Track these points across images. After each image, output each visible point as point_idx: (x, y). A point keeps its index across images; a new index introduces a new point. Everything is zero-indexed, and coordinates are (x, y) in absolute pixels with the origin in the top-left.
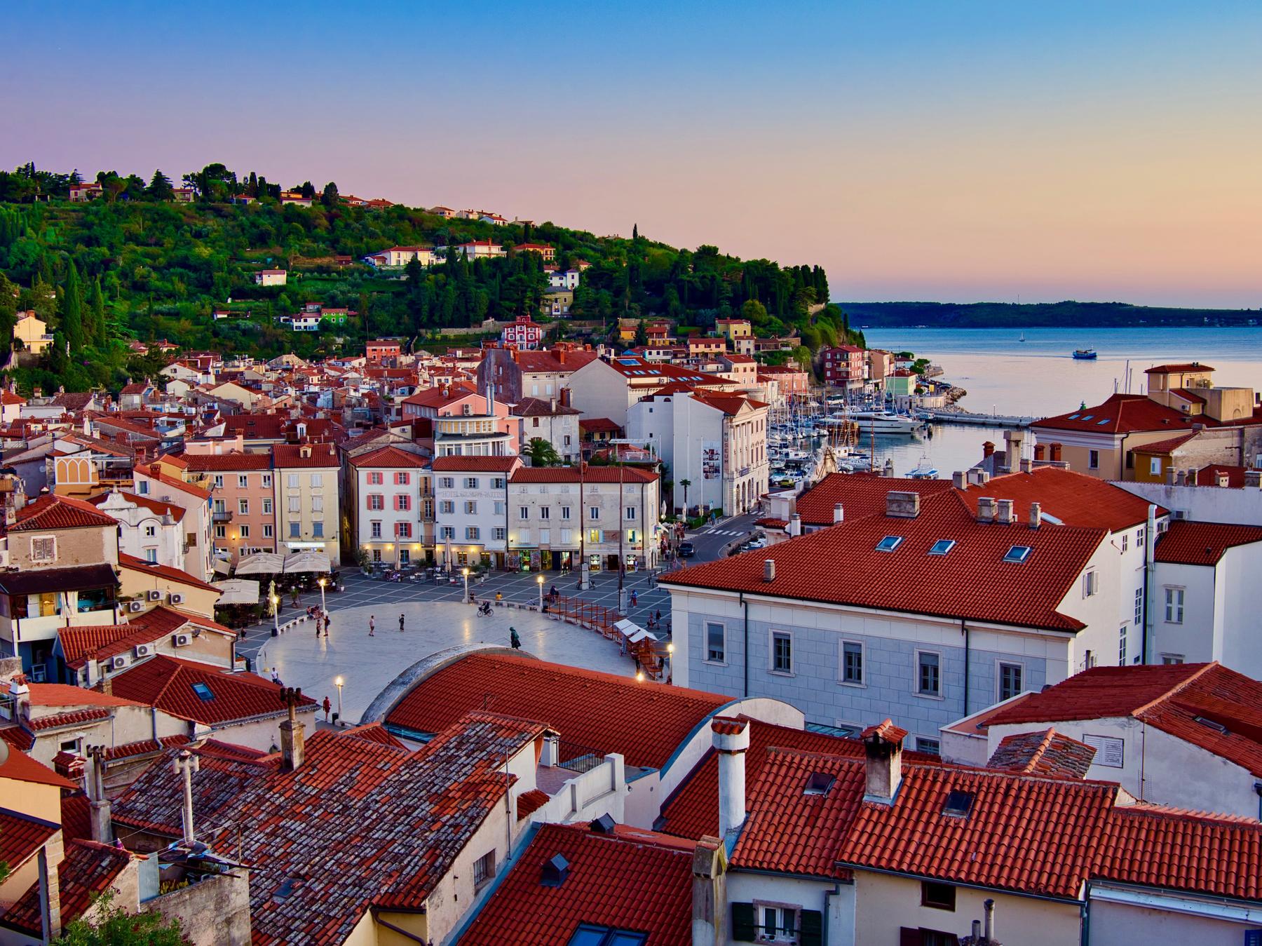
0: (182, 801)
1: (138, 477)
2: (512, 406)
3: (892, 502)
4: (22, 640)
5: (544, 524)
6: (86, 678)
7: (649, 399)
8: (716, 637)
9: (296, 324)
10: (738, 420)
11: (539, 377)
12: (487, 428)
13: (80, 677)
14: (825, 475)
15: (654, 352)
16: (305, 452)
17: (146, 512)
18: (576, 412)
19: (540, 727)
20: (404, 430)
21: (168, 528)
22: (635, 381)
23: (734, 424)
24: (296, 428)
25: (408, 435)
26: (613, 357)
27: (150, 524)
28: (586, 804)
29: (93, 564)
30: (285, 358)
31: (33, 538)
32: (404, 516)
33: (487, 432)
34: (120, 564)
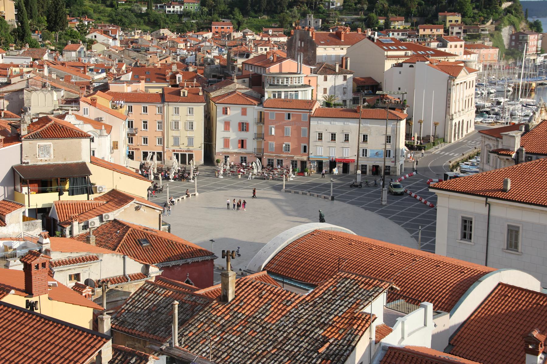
0: (171, 321)
1: (83, 105)
2: (313, 67)
4: (31, 207)
5: (332, 144)
6: (71, 232)
7: (400, 65)
9: (167, 9)
10: (457, 81)
11: (327, 49)
12: (297, 81)
13: (67, 232)
14: (540, 121)
15: (396, 33)
16: (184, 93)
19: (388, 284)
20: (244, 81)
21: (103, 138)
23: (456, 83)
28: (409, 335)
29: (75, 162)
30: (162, 31)
31: (38, 144)
32: (243, 135)
33: (297, 84)
34: (91, 162)
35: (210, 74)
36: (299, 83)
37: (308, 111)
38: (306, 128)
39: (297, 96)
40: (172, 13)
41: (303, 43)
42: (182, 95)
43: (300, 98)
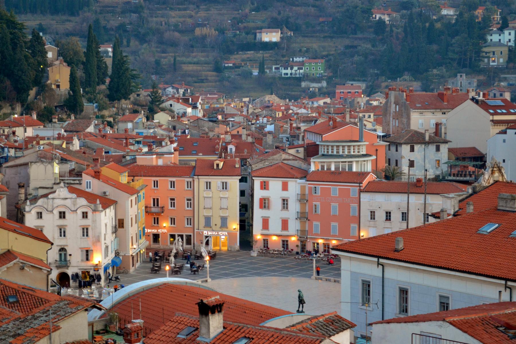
1: (86, 178)
3: (503, 199)
8: (366, 286)
9: (284, 71)
12: (356, 150)
14: (492, 182)
16: (218, 165)
17: (82, 201)
18: (446, 142)
20: (298, 151)
21: (97, 214)
22: (496, 118)
24: (227, 147)
25: (301, 155)
26: (481, 98)
27: (85, 210)
33: (356, 153)
35: (273, 145)
36: (359, 152)
37: (358, 185)
38: (356, 205)
39: (350, 167)
40: (289, 75)
41: (397, 107)
42: (215, 167)
43: (354, 169)
